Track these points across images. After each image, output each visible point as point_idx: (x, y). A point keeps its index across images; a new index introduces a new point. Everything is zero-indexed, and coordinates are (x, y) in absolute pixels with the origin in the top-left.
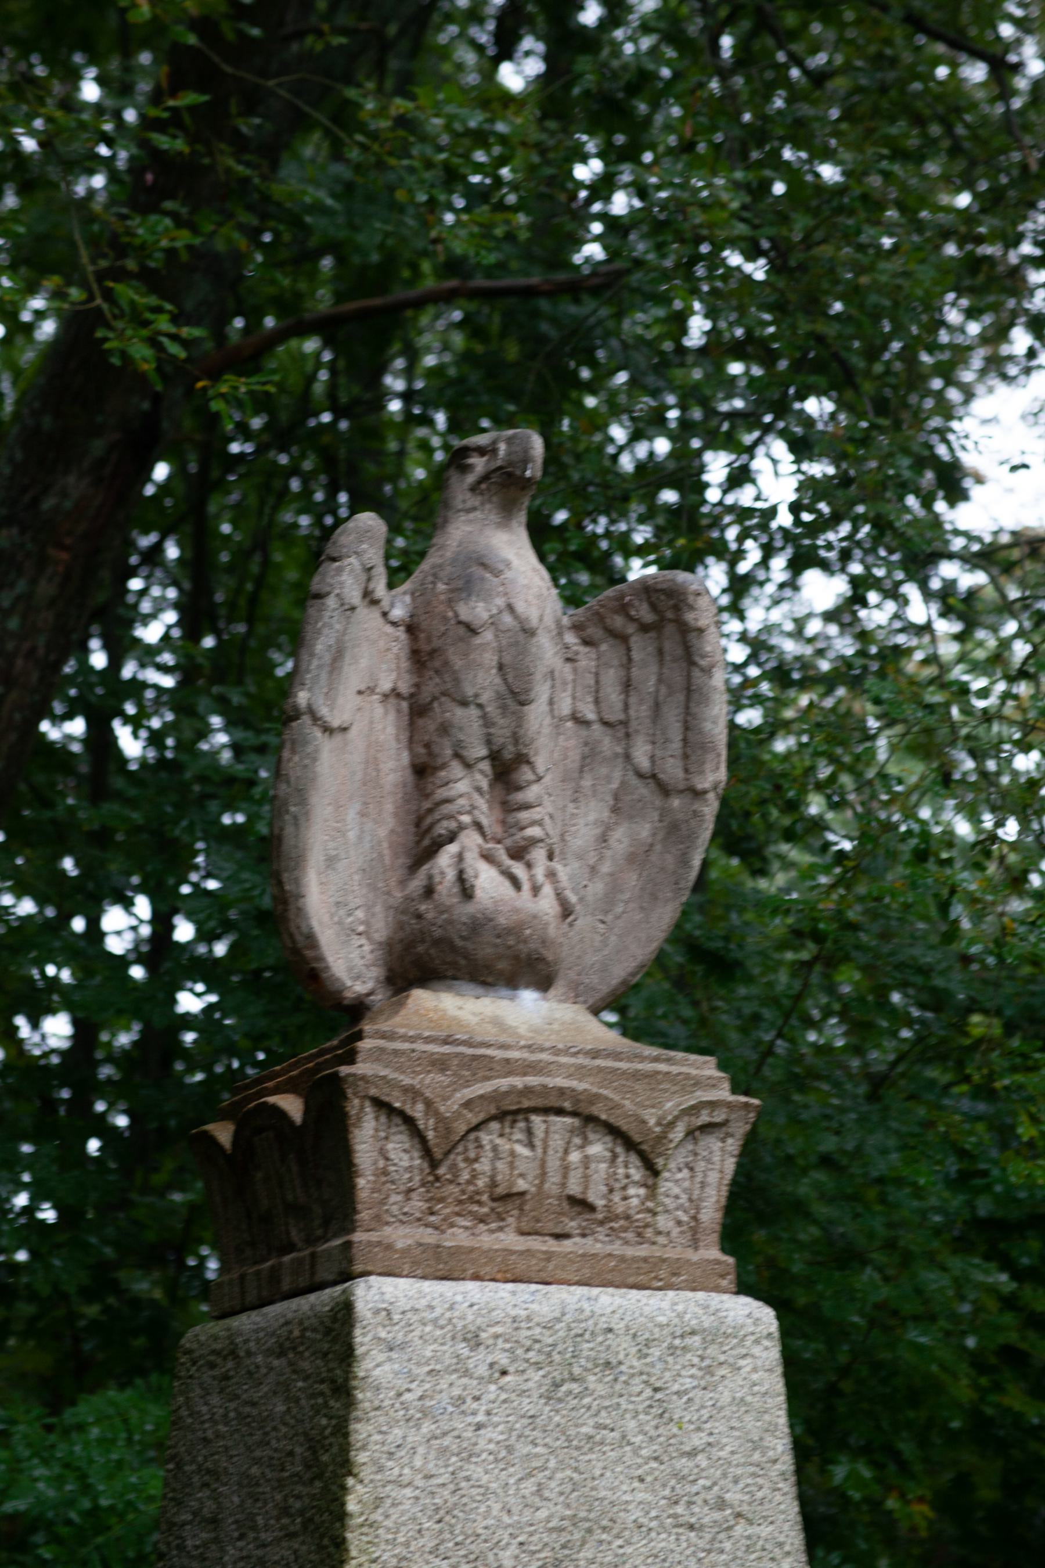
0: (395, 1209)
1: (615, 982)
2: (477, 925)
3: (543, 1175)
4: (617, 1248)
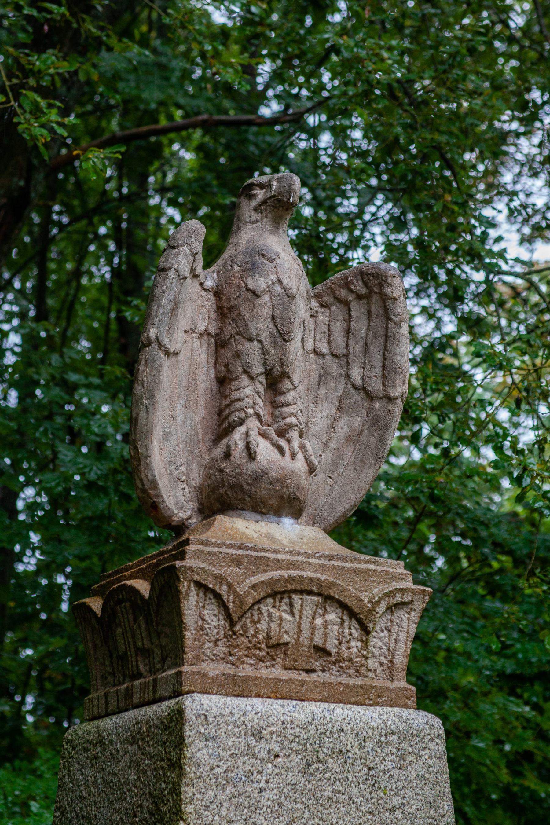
0: (208, 652)
1: (337, 515)
2: (257, 477)
3: (300, 631)
4: (344, 679)
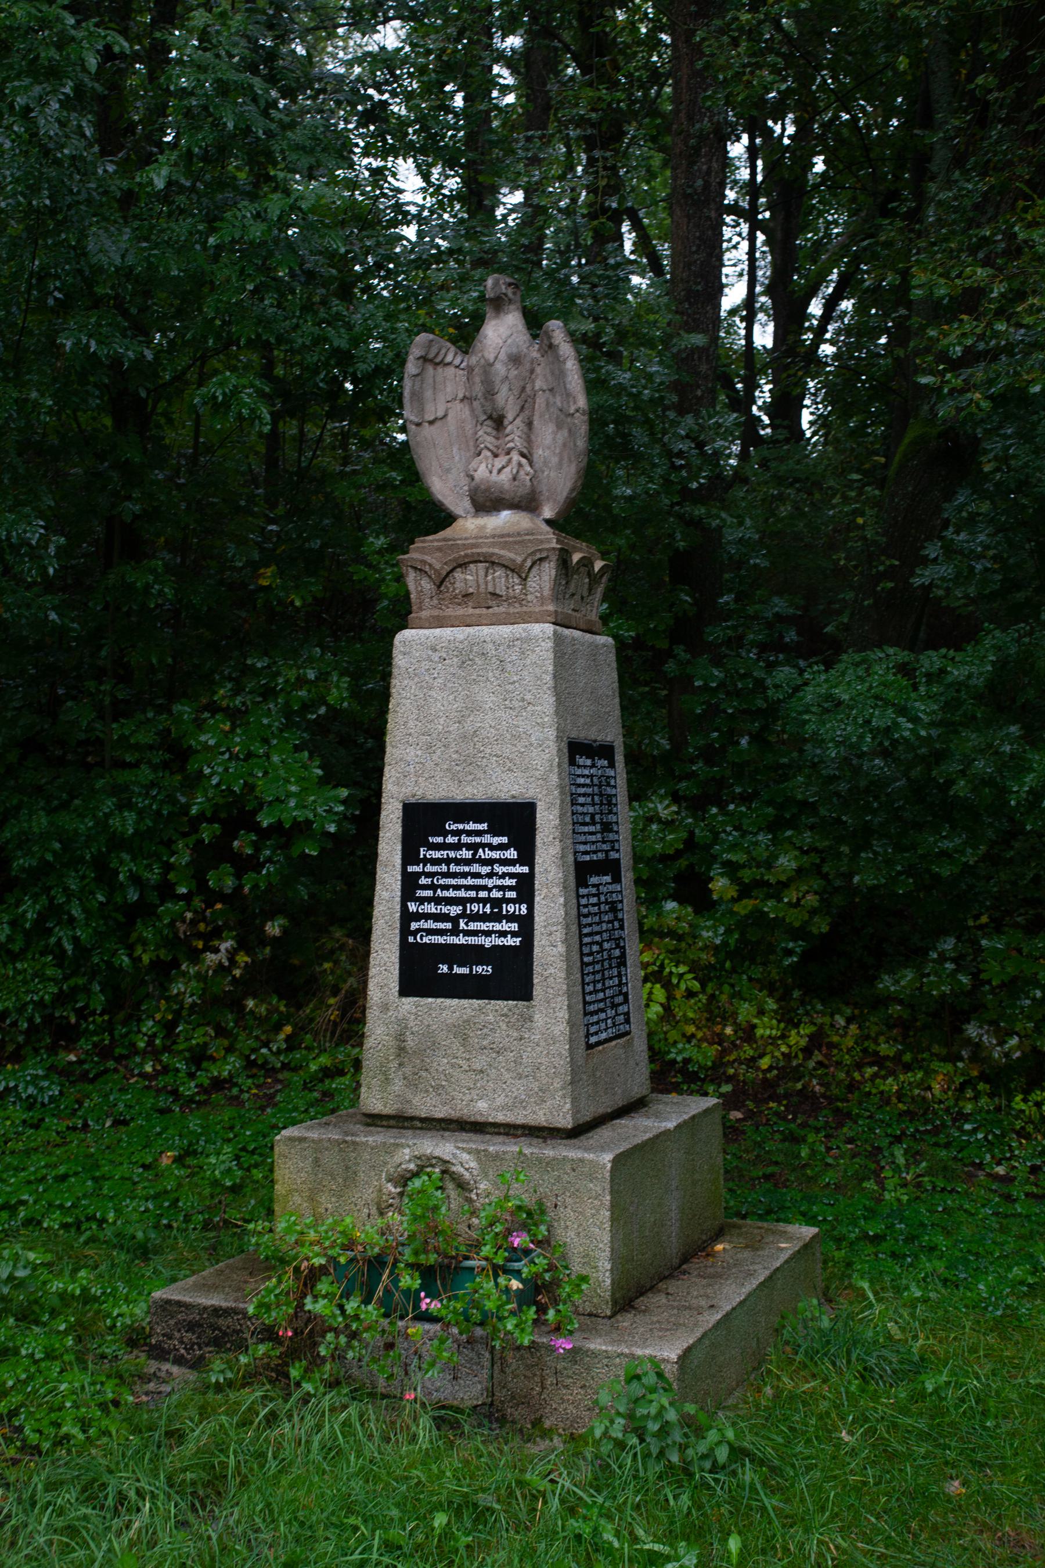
3: (478, 586)
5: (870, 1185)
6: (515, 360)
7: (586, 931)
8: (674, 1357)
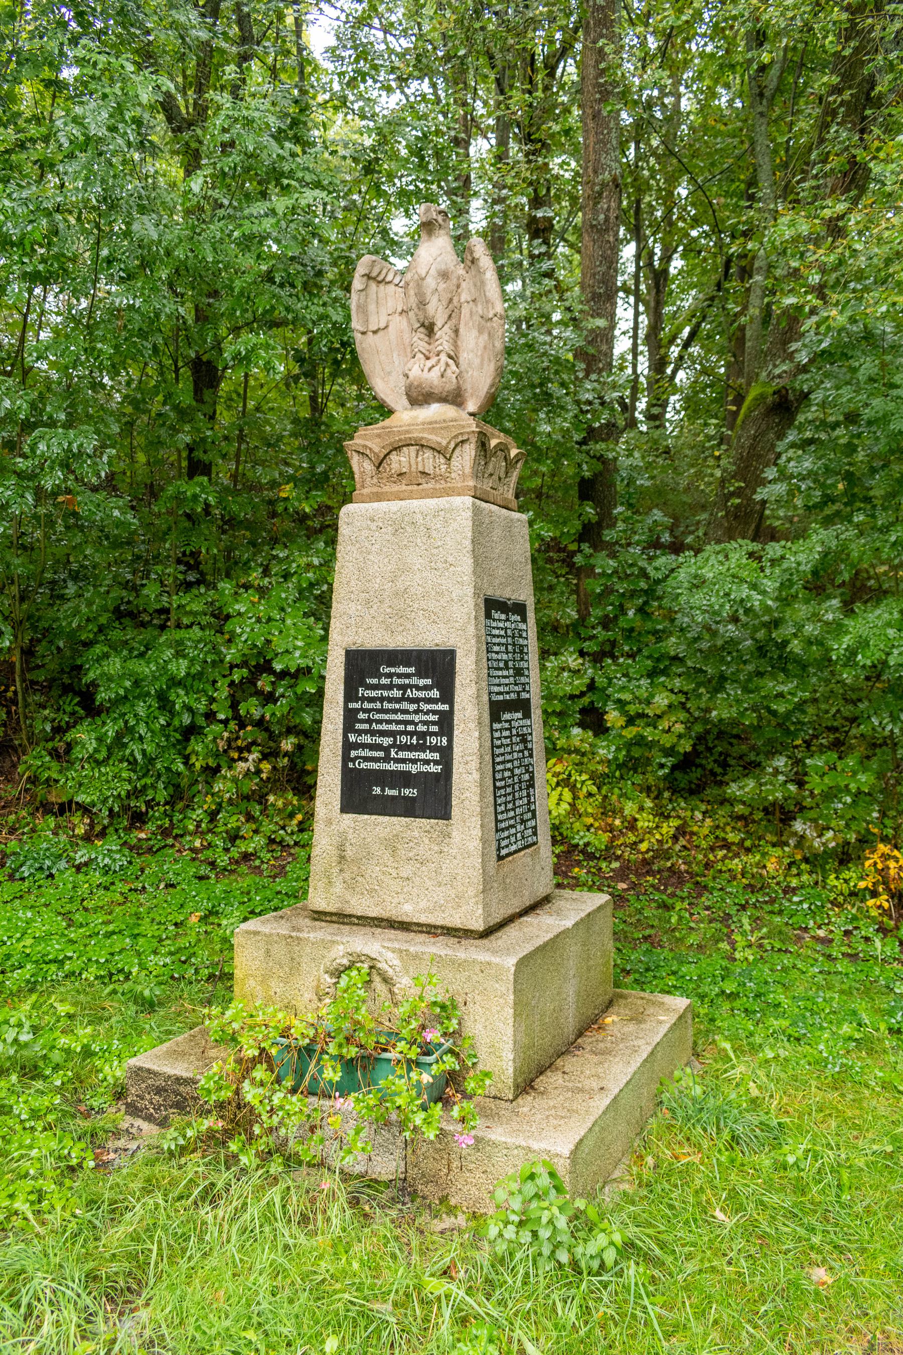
5: (724, 946)
6: (444, 275)
7: (498, 760)
8: (566, 1152)
